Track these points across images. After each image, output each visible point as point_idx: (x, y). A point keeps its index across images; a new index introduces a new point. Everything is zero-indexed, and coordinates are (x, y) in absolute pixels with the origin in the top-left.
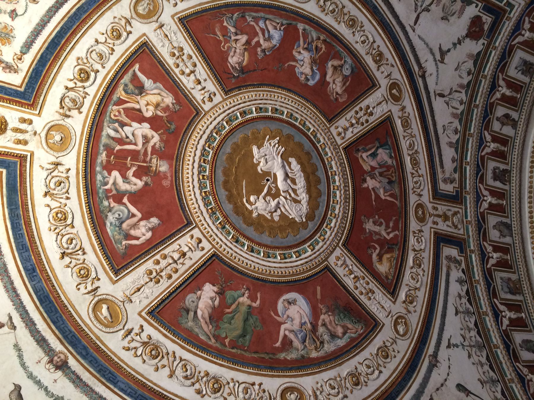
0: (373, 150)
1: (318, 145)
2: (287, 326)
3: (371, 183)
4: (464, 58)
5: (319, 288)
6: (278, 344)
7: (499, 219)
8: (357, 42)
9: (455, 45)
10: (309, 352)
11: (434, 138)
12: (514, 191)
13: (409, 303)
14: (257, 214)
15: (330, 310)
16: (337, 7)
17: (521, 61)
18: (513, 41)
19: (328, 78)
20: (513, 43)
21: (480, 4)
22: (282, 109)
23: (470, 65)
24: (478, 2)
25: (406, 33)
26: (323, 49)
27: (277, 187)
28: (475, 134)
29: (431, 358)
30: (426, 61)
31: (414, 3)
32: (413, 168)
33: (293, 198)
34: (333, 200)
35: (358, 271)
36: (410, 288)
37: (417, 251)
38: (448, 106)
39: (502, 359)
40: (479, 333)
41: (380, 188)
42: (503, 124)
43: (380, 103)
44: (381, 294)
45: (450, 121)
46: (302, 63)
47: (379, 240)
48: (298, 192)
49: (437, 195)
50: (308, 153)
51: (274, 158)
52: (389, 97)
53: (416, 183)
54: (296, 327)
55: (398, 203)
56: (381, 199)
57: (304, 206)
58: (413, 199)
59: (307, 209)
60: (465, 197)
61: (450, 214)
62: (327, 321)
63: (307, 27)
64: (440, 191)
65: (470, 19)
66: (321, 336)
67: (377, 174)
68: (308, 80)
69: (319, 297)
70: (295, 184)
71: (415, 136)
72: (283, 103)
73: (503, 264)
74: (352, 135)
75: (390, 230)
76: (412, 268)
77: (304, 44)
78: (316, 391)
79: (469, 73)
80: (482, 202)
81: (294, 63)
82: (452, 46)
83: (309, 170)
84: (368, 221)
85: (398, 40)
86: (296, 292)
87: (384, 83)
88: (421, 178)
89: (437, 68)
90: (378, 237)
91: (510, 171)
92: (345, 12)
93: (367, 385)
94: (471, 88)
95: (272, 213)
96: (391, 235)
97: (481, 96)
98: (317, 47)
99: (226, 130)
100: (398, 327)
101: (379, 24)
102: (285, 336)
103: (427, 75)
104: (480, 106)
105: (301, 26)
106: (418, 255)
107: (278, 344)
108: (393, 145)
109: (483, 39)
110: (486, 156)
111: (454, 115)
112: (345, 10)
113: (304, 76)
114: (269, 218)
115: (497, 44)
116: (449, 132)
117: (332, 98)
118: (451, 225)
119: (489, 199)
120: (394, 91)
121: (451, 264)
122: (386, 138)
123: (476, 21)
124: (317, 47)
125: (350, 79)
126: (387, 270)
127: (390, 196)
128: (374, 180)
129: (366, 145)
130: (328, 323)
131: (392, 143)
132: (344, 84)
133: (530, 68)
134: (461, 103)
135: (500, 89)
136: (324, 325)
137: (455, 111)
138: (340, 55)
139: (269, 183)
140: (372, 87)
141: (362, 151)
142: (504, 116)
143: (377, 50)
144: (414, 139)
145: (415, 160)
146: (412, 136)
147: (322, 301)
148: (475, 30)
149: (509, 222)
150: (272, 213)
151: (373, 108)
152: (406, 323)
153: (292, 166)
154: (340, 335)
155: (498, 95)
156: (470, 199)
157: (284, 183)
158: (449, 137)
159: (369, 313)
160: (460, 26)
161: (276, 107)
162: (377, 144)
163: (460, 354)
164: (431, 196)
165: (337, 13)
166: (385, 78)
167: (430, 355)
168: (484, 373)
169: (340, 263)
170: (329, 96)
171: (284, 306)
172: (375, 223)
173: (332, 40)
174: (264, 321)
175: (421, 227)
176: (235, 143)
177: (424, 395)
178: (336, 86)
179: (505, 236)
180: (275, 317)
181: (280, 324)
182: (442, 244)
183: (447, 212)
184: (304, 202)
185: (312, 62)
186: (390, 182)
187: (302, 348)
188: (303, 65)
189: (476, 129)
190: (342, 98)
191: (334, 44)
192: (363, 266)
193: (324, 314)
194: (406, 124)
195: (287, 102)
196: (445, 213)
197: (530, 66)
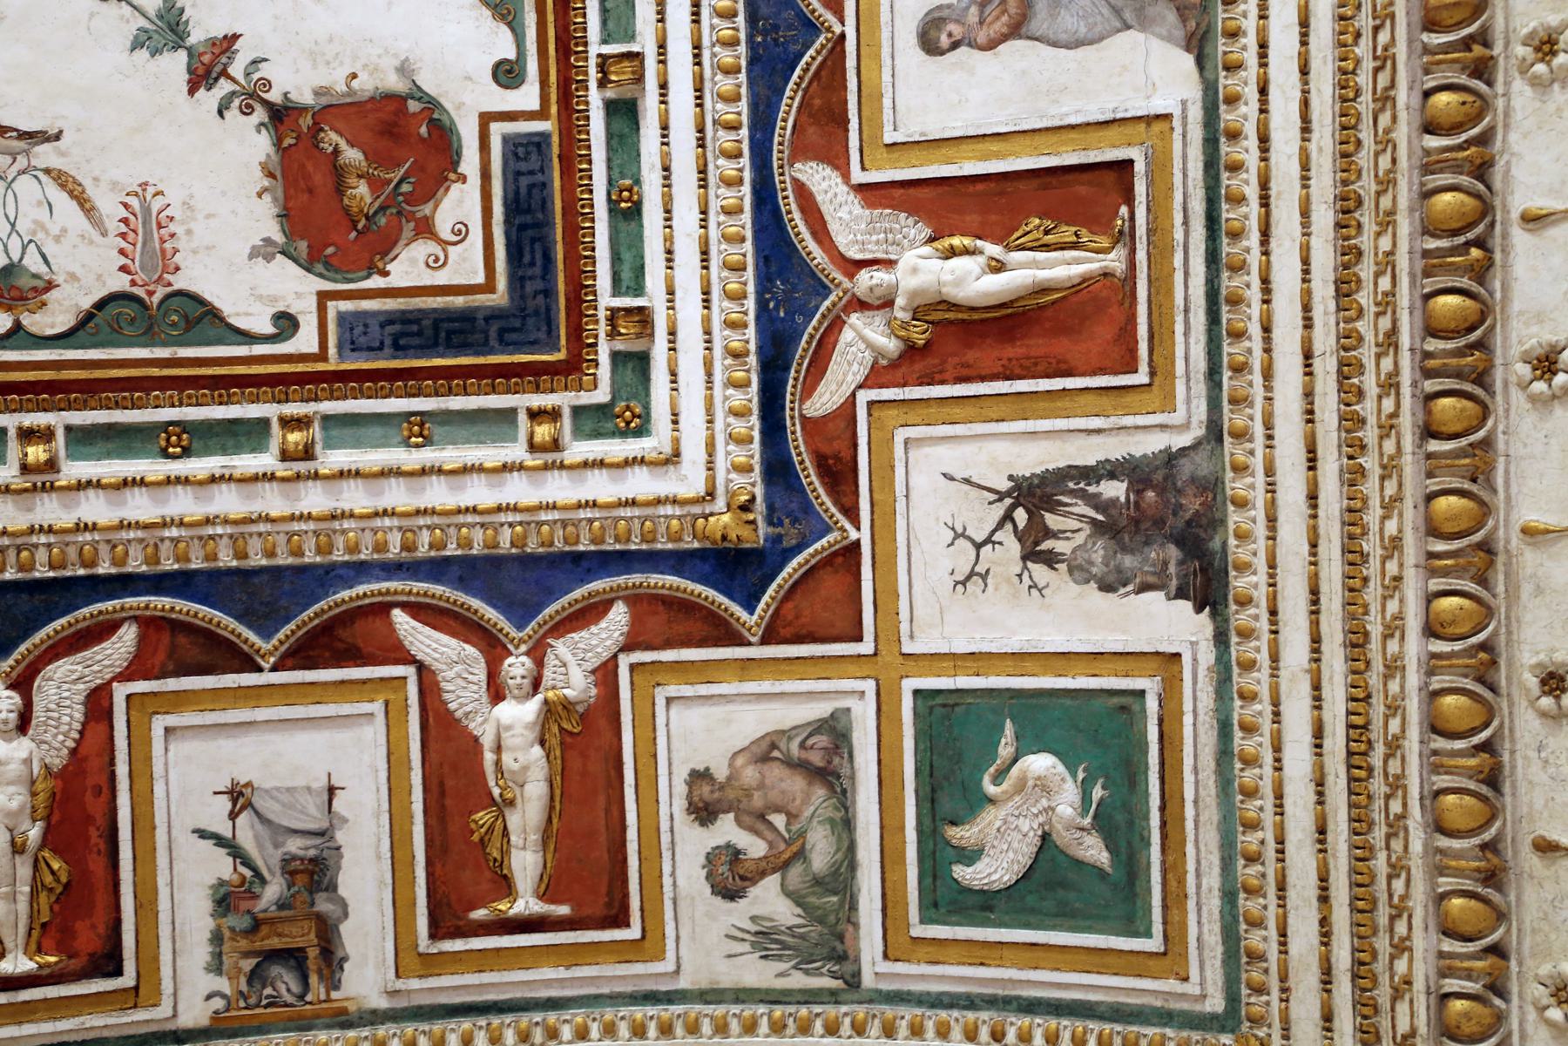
17: (313, 818)
18: (422, 611)
21: (527, 97)
109: (323, 297)
115: (334, 459)
123: (406, 132)
133: (293, 957)
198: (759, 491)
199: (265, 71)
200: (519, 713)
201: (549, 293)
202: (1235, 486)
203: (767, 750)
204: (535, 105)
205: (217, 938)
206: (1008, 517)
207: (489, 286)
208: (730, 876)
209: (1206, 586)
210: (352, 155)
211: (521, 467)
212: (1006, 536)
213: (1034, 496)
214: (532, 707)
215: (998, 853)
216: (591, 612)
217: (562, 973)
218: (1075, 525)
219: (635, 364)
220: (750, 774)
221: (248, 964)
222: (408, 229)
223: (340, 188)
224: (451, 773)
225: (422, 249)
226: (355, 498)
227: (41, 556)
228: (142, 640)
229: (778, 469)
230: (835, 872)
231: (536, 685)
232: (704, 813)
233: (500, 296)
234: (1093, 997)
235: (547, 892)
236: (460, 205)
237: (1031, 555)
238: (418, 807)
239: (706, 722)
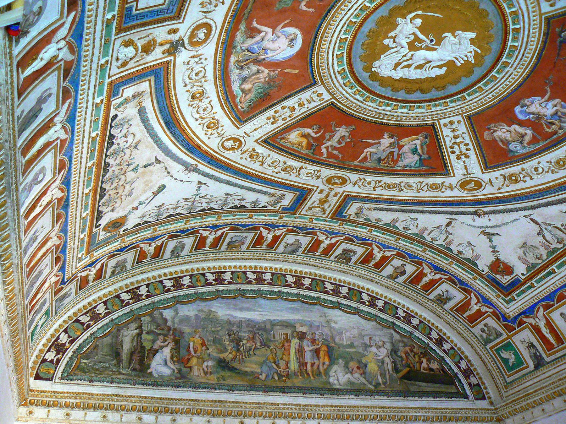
0: (420, 151)
2: (270, 36)
3: (386, 141)
4: (477, 251)
5: (296, 72)
6: (255, 24)
8: (539, 163)
9: (494, 247)
10: (236, 54)
12: (326, 263)
13: (251, 154)
14: (400, 22)
15: (271, 80)
18: (474, 294)
19: (515, 127)
20: (472, 294)
21: (523, 278)
23: (468, 254)
24: (526, 276)
25: (526, 209)
26: (547, 130)
27: (421, 48)
28: (397, 244)
29: (195, 166)
30: (490, 220)
33: (402, 63)
34: (382, 102)
35: (299, 112)
36: (265, 158)
37: (299, 171)
39: (174, 225)
40: (204, 210)
42: (396, 268)
44: (269, 130)
46: (543, 105)
47: (324, 138)
49: (348, 199)
50: (443, 88)
51: (453, 53)
52: (469, 179)
53: (369, 183)
54: (266, 44)
58: (354, 177)
60: (337, 223)
61: (326, 206)
62: (261, 75)
65: (514, 266)
66: (248, 68)
68: (522, 107)
69: (288, 71)
70: (416, 68)
71: (418, 191)
73: (259, 241)
75: (330, 149)
76: (285, 163)
77: (562, 113)
78: (198, 58)
79: (459, 252)
80: (327, 235)
81: (546, 97)
82: (494, 244)
83: (425, 85)
85: (522, 200)
86: (301, 49)
87: (486, 177)
89: (478, 227)
90: (327, 137)
91: (347, 264)
93: (189, 105)
94: (445, 251)
95: (394, 38)
96: (324, 150)
98: (553, 124)
99: (507, 9)
100: (232, 142)
101: (548, 188)
102: (260, 32)
104: (423, 254)
106: (295, 171)
107: (255, 24)
108: (418, 171)
111: (424, 230)
113: (528, 103)
114: (390, 35)
115: (478, 282)
116: (408, 223)
117: (493, 125)
119: (327, 242)
120: (473, 184)
121: (276, 198)
123: (509, 270)
124: (553, 124)
125: (504, 147)
126: (290, 140)
129: (428, 146)
130: (258, 76)
132: (502, 141)
133: (442, 302)
136: (258, 72)
137: (428, 232)
139: (429, 42)
140: (486, 166)
141: (424, 141)
142: (405, 270)
143: (522, 179)
145: (393, 187)
147: (282, 74)
148: (500, 266)
149: (297, 253)
150: (394, 38)
151: (464, 162)
152: (233, 148)
154: (243, 87)
156: (334, 226)
157: (422, 58)
159: (254, 116)
160: (510, 256)
162: (424, 157)
163: (189, 190)
164: (350, 194)
166: (490, 179)
167: (197, 166)
168: (168, 209)
169: (315, 97)
170: (496, 123)
171: (291, 35)
172: (343, 137)
173: (553, 141)
174: (283, 11)
176: (488, 15)
177: (165, 157)
180: (283, 24)
181: (274, 28)
182: (298, 193)
185: (540, 115)
186: (380, 160)
187: (243, 48)
188: (541, 106)
190: (488, 134)
191: (547, 142)
192: (303, 118)
193: (268, 74)
194: (434, 187)
196: (328, 201)
200: (476, 308)
202: (545, 367)
203: (495, 329)
208: (483, 330)
209: (537, 367)
210: (502, 266)
214: (477, 308)
215: (505, 355)
225: (502, 277)
229: (516, 318)
236: (509, 278)
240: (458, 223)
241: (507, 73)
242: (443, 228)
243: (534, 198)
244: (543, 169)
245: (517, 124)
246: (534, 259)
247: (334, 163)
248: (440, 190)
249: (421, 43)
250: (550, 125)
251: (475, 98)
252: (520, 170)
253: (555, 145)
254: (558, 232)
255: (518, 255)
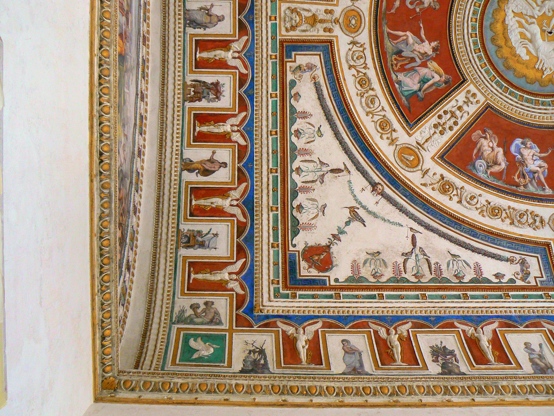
0: (426, 86)
1: (498, 78)
3: (427, 47)
7: (208, 31)
9: (342, 232)
11: (335, 117)
16: (519, 221)
18: (244, 264)
19: (501, 150)
21: (333, 283)
22: (545, 107)
23: (303, 218)
25: (420, 223)
31: (428, 255)
32: (365, 74)
38: (320, 161)
41: (413, 44)
43: (426, 141)
45: (312, 143)
46: (535, 158)
48: (517, 25)
51: (546, 56)
52: (416, 150)
55: (386, 29)
56: (412, 32)
57: (511, 11)
58: (364, 37)
59: (508, 8)
63: (542, 193)
64: (319, 53)
67: (417, 59)
68: (522, 143)
70: (521, 34)
72: (545, 113)
74: (456, 98)
77: (538, 176)
79: (300, 207)
81: (543, 155)
82: (346, 229)
83: (505, 51)
84: (430, 4)
85: (428, 213)
88: (352, 63)
91: (184, 101)
92: (507, 219)
94: (286, 193)
97: (268, 185)
98: (524, 177)
101: (463, 221)
103: (370, 188)
104: (265, 173)
105: (549, 191)
109: (299, 251)
110: (237, 112)
111: (306, 152)
112: (508, 221)
113: (528, 146)
117: (490, 132)
118: (302, 12)
120: (412, 158)
122: (409, 104)
123: (327, 264)
124: (524, 177)
125: (474, 157)
127: (398, 37)
128: (422, 51)
129: (437, 89)
131: (400, 99)
132: (479, 150)
133: (188, 241)
134: (298, 170)
135: (235, 203)
137: (307, 158)
138: (494, 178)
142: (213, 172)
144: (368, 110)
146: (371, 113)
153: (525, 50)
155: (236, 194)
158: (309, 124)
161: (551, 108)
162: (420, 94)
165: (516, 215)
173: (509, 189)
175: (353, 5)
178: (488, 145)
179: (201, 9)
183: (308, 28)
184: (510, 15)
185: (524, 162)
186: (399, 53)
188: (533, 156)
189: (265, 142)
190: (478, 134)
191: (505, 186)
194: (384, 125)
195: (540, 115)
196: (312, 26)
197: (191, 244)
198: (263, 314)
199: (335, 245)
200: (226, 277)
201: (299, 284)
203: (217, 313)
204: (331, 284)
205: (193, 231)
206: (257, 348)
207: (300, 276)
208: (194, 307)
210: (322, 257)
211: (269, 278)
212: (254, 348)
213: (262, 352)
216: (243, 288)
217: (180, 281)
218: (256, 357)
219: (287, 296)
220: (212, 311)
221: (188, 235)
222: (310, 264)
223: (317, 255)
224: (216, 266)
225: (307, 266)
226: (265, 253)
227: (258, 209)
228: (243, 223)
229: (267, 317)
230: (193, 322)
231: (231, 280)
232: (206, 303)
233: (298, 277)
234: (168, 355)
235: (194, 279)
236: (314, 272)
237: (250, 352)
238: (212, 261)
239: (222, 305)
240: (347, 178)
241: (545, 109)
242: (325, 169)
243: (440, 220)
244: (478, 202)
245: (504, 151)
246: (369, 273)
247: (381, 9)
248: (382, 134)
249: (547, 24)
250: (521, 176)
251: (511, 99)
252: (460, 187)
253: (507, 193)
254: (425, 267)
255: (356, 258)
